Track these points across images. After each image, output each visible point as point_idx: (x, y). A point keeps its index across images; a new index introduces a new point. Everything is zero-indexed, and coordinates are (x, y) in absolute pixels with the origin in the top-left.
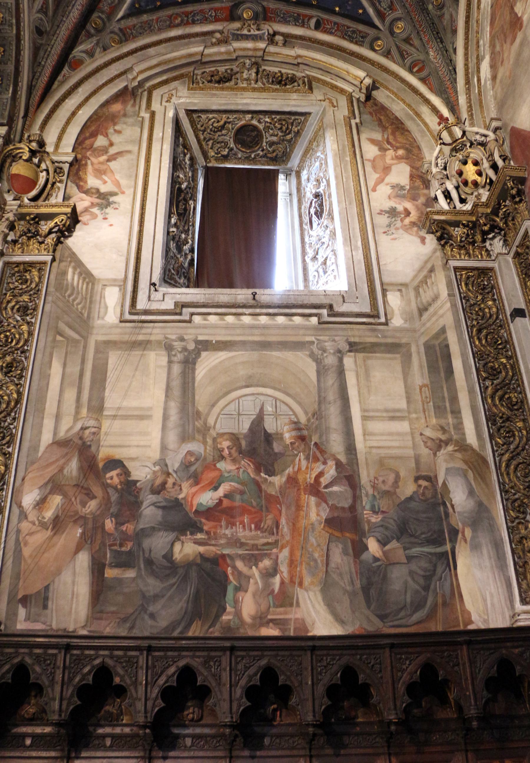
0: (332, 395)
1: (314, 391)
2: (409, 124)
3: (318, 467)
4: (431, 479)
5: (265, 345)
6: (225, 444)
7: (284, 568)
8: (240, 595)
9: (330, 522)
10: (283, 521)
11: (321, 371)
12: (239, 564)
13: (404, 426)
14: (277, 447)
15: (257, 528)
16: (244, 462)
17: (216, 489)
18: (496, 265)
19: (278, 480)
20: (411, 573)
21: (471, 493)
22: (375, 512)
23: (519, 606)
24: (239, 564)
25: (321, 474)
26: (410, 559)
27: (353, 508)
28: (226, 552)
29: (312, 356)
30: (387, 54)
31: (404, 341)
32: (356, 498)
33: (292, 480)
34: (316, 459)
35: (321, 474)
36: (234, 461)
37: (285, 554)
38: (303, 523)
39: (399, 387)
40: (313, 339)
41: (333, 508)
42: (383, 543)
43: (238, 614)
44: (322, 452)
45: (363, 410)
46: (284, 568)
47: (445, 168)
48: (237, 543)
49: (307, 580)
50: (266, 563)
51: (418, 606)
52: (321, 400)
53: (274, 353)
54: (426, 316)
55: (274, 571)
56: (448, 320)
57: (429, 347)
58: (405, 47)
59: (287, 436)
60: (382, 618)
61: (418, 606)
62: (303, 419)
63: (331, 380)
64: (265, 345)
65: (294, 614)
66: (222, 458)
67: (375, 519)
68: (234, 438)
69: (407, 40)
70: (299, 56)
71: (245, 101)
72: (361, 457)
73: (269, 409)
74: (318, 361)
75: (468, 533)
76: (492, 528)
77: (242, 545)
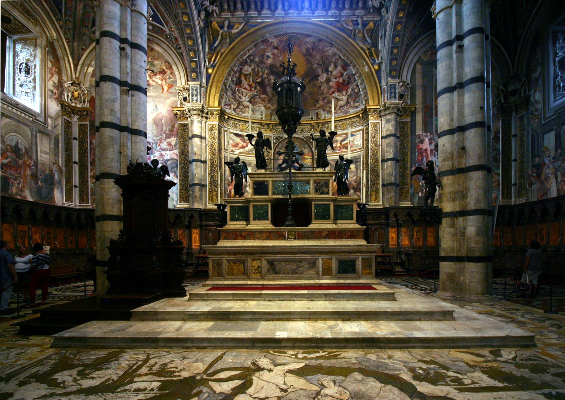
0: (34, 143)
1: (30, 140)
2: (61, 61)
3: (30, 161)
4: (52, 171)
5: (19, 121)
6: (9, 148)
7: (22, 183)
8: (13, 188)
9: (32, 175)
10: (22, 172)
11: (32, 135)
12: (12, 180)
13: (47, 157)
14: (21, 153)
15: (16, 172)
16: (13, 154)
17: (6, 159)
18: (73, 122)
19: (21, 162)
20: (46, 191)
21: (59, 177)
22: (41, 175)
23: (64, 202)
24: (12, 180)
25: (30, 163)
26: (46, 187)
27: (36, 173)
28: (9, 176)
29: (30, 130)
30: (61, 28)
31: (50, 134)
32: (37, 171)
33: (24, 163)
34: (29, 159)
35: (30, 163)
36: (11, 153)
37: (22, 180)
38: (26, 174)
39: (48, 146)
40: (29, 124)
41: (32, 172)
42: (42, 183)
43: (12, 191)
44: (31, 157)
45: (40, 150)
46: (22, 183)
47: (69, 87)
48: (11, 174)
49: (27, 187)
50: (18, 181)
51: (47, 197)
52: (32, 144)
53: (21, 125)
54: (56, 129)
55: (19, 184)
56: (60, 132)
57: (55, 138)
58: (67, 30)
59: (23, 150)
60: (40, 198)
61: (47, 197)
62: (27, 147)
63: (34, 139)
64: (19, 121)
65: (23, 194)
66: (8, 151)
67: (41, 177)
68: (11, 146)
69: (69, 30)
70: (37, 9)
71: (16, 15)
72: (39, 161)
73: (19, 141)
74: (32, 132)
75: (57, 185)
76: (61, 185)
77: (13, 176)
